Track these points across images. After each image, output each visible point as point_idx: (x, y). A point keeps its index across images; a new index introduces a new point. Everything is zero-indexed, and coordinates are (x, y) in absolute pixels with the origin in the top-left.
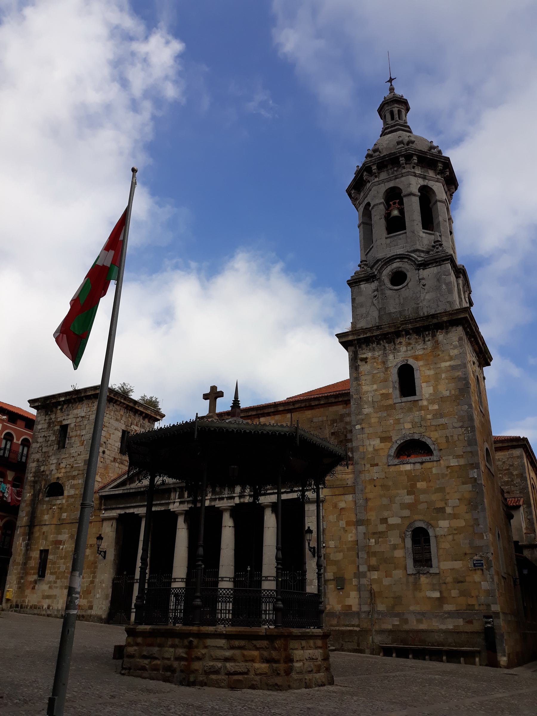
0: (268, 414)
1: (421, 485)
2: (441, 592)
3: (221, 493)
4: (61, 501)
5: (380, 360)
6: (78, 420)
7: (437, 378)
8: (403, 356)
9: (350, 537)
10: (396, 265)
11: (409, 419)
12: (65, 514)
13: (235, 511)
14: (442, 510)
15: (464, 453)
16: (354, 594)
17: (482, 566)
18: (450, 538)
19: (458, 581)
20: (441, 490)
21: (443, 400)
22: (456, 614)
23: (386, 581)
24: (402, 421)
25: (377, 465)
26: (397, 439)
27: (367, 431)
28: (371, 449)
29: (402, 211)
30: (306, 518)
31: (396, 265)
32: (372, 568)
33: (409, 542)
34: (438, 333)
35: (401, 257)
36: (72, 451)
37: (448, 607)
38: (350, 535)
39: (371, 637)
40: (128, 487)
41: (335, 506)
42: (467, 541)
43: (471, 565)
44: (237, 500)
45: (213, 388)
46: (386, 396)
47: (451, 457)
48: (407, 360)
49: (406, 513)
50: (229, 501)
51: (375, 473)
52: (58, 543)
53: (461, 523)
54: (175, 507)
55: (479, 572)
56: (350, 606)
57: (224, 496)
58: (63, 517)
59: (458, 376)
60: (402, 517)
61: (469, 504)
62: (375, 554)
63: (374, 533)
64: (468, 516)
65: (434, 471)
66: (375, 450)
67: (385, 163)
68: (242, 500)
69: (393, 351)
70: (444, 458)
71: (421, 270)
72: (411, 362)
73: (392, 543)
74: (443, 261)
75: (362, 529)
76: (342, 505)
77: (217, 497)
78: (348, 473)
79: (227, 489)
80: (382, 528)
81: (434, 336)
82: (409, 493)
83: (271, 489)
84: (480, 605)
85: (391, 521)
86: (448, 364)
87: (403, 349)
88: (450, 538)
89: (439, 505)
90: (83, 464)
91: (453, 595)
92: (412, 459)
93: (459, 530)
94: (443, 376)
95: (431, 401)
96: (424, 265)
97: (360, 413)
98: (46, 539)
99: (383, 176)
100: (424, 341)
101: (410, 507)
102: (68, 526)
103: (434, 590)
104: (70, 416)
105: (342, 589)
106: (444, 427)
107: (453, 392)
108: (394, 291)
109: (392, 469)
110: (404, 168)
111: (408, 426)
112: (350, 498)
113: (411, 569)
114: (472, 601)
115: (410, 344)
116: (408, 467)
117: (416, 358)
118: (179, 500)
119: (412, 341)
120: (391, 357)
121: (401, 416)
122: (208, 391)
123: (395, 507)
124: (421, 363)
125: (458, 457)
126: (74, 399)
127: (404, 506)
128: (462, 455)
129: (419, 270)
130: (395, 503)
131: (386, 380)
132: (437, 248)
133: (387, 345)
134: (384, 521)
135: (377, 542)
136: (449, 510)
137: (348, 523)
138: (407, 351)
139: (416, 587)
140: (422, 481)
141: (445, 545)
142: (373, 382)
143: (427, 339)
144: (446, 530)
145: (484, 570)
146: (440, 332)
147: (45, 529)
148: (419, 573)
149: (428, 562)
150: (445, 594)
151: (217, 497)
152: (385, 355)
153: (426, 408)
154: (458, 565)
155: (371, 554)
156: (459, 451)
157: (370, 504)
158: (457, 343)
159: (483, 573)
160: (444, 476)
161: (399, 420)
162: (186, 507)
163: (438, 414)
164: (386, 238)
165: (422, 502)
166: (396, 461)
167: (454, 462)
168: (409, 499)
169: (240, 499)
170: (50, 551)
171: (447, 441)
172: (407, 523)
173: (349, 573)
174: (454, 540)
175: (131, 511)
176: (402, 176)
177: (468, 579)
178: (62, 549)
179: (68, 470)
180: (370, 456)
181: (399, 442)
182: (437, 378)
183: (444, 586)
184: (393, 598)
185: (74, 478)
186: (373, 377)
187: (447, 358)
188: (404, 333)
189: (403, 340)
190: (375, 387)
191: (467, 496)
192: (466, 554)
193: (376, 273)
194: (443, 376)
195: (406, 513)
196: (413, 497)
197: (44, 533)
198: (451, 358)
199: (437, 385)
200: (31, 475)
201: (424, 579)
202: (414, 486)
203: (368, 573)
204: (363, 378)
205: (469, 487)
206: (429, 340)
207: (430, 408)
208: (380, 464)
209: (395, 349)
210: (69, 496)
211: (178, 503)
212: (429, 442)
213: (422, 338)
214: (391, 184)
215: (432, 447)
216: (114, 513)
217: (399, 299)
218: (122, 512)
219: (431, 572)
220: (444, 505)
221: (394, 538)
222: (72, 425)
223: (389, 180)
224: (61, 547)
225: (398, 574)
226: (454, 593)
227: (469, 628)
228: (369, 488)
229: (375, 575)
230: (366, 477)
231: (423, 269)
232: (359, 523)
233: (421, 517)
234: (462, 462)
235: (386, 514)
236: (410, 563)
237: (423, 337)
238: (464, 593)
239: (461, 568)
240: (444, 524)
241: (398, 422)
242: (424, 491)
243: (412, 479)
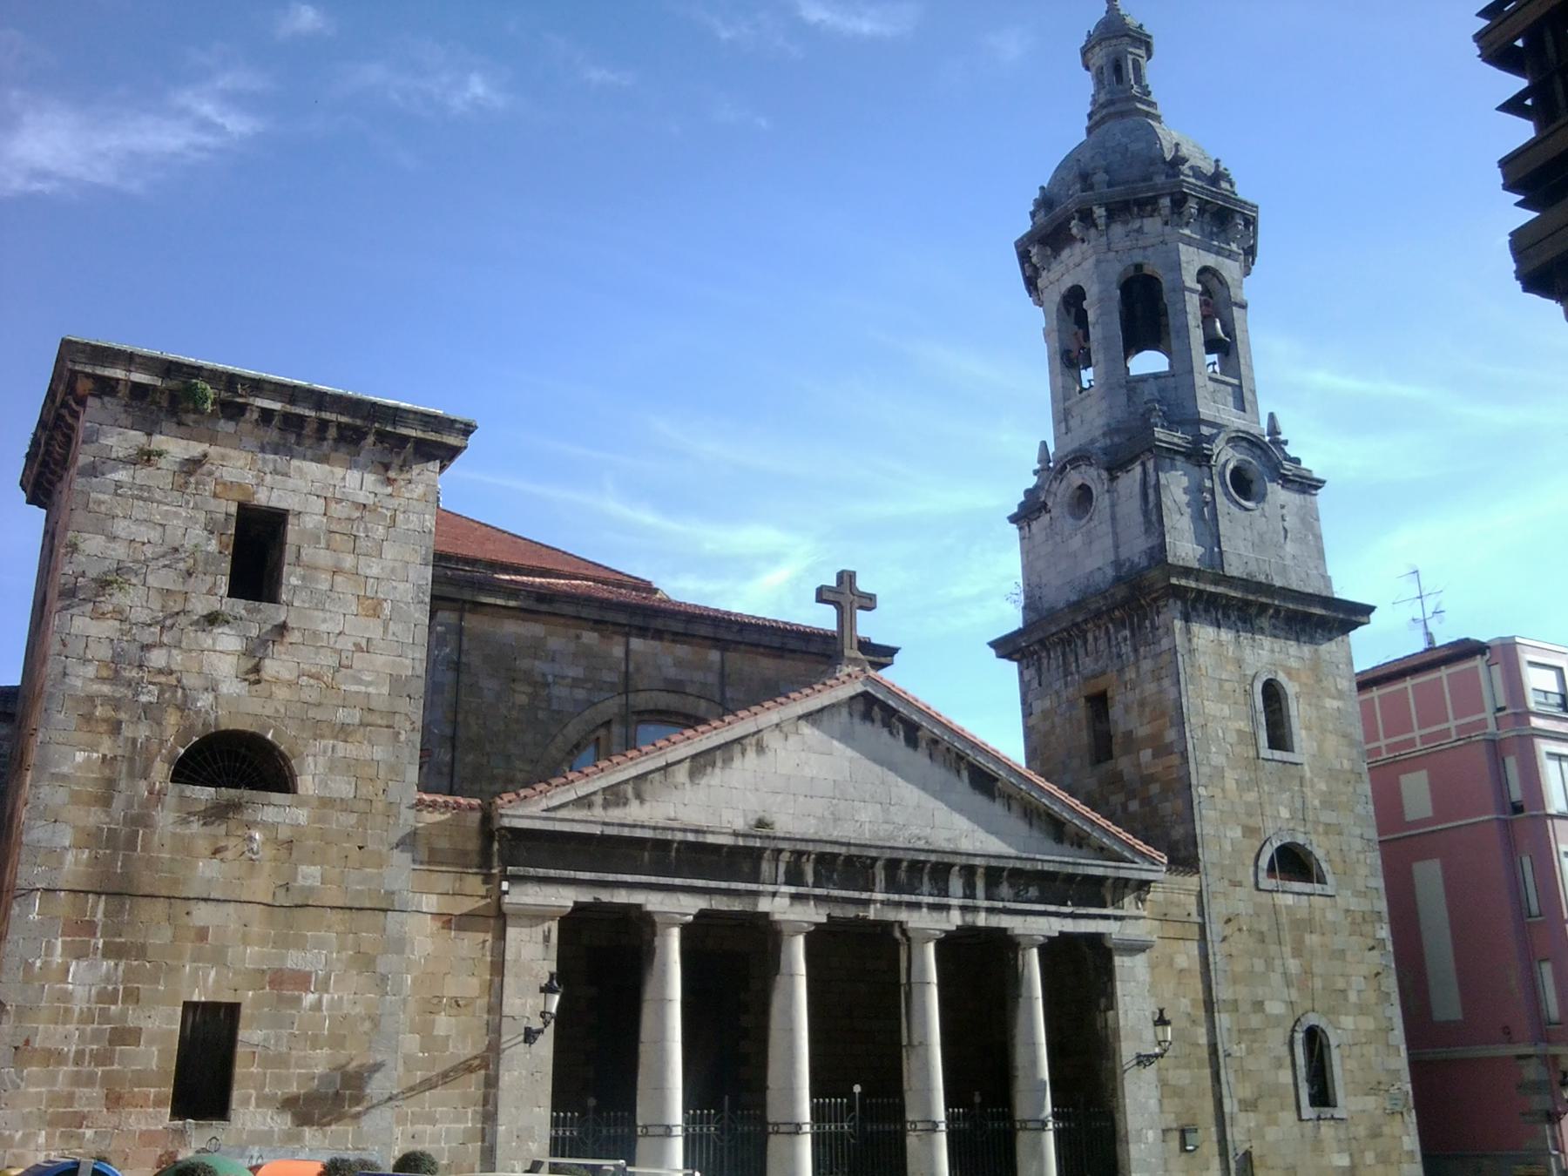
0: (659, 635)
4: (273, 811)
6: (337, 510)
12: (315, 870)
13: (949, 946)
19: (1375, 1134)
21: (1333, 775)
30: (1118, 984)
32: (1248, 1106)
36: (324, 627)
40: (598, 813)
44: (955, 920)
45: (847, 578)
50: (935, 915)
52: (285, 983)
54: (778, 905)
58: (300, 881)
68: (969, 918)
72: (1282, 677)
77: (906, 898)
79: (926, 879)
80: (1255, 1021)
89: (1341, 984)
90: (385, 690)
98: (218, 957)
102: (335, 916)
104: (291, 483)
116: (1289, 899)
118: (793, 890)
122: (863, 585)
126: (323, 425)
134: (1258, 1005)
135: (1250, 1051)
136: (1353, 997)
139: (1317, 1145)
147: (203, 915)
148: (1319, 1118)
151: (906, 898)
154: (1371, 1102)
162: (815, 915)
167: (1355, 904)
168: (1293, 965)
169: (963, 915)
170: (245, 1011)
175: (621, 897)
178: (317, 1006)
179: (310, 695)
185: (343, 732)
186: (1221, 687)
197: (202, 934)
200: (91, 671)
201: (1326, 1130)
203: (1241, 1117)
210: (326, 803)
211: (787, 901)
216: (565, 898)
218: (586, 896)
222: (311, 522)
224: (309, 999)
226: (1370, 1157)
235: (1260, 992)
240: (1348, 1022)
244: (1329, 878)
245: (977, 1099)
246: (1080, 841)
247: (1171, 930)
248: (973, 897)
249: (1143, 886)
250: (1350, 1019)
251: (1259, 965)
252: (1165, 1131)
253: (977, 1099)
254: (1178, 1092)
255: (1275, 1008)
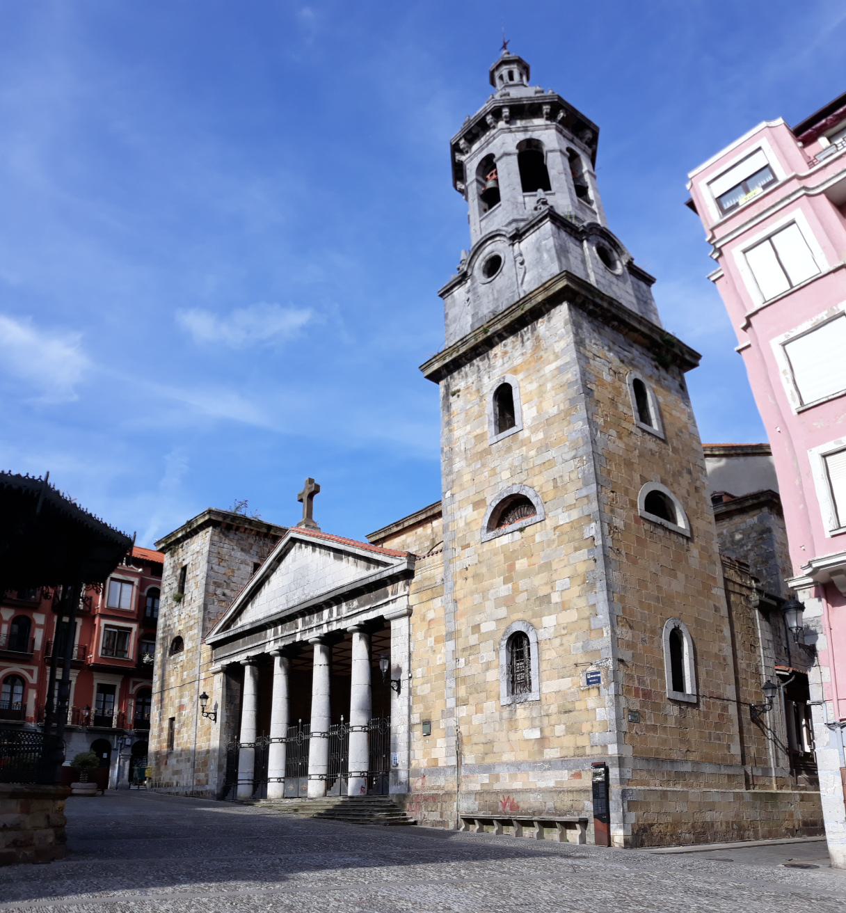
1: (521, 564)
2: (542, 731)
3: (311, 622)
5: (474, 389)
7: (541, 392)
8: (500, 373)
9: (439, 659)
10: (489, 249)
11: (506, 464)
14: (547, 598)
15: (577, 500)
16: (441, 742)
17: (599, 682)
18: (557, 642)
20: (547, 566)
22: (563, 762)
23: (477, 719)
24: (498, 470)
25: (468, 546)
26: (492, 500)
27: (457, 497)
28: (462, 524)
29: (496, 180)
31: (489, 249)
32: (461, 702)
33: (504, 656)
34: (539, 325)
35: (492, 237)
37: (551, 754)
38: (439, 656)
39: (455, 804)
41: (423, 619)
42: (580, 644)
43: (583, 682)
44: (325, 630)
46: (480, 438)
47: (560, 510)
48: (504, 378)
49: (502, 612)
51: (466, 558)
53: (571, 616)
55: (594, 692)
56: (436, 760)
57: (313, 626)
59: (567, 380)
60: (498, 620)
61: (584, 583)
62: (464, 679)
63: (464, 650)
64: (582, 603)
65: (538, 539)
66: (467, 524)
67: (474, 131)
69: (488, 370)
70: (550, 515)
71: (517, 244)
73: (484, 661)
74: (541, 221)
75: (451, 645)
76: (431, 615)
78: (436, 567)
80: (473, 639)
81: (534, 330)
82: (506, 581)
83: (358, 607)
84: (592, 746)
85: (485, 628)
86: (554, 366)
87: (498, 362)
88: (557, 642)
91: (557, 734)
92: (508, 528)
93: (568, 629)
94: (549, 386)
95: (534, 430)
96: (517, 237)
97: (450, 472)
99: (475, 147)
100: (523, 342)
101: (508, 602)
103: (533, 727)
105: (429, 735)
106: (549, 464)
107: (562, 407)
108: (487, 285)
109: (487, 546)
110: (494, 127)
111: (506, 475)
112: (438, 602)
113: (506, 700)
114: (583, 741)
115: (505, 353)
116: (505, 540)
117: (515, 371)
119: (509, 348)
120: (485, 380)
121: (496, 463)
123: (489, 605)
124: (520, 376)
125: (570, 507)
127: (500, 602)
128: (575, 504)
129: (513, 245)
130: (488, 600)
131: (480, 415)
132: (540, 209)
133: (480, 364)
134: (476, 628)
136: (555, 598)
137: (437, 641)
138: (504, 364)
140: (522, 558)
141: (550, 654)
142: (467, 422)
143: (525, 338)
144: (552, 630)
145: (602, 688)
146: (541, 322)
149: (526, 684)
150: (547, 733)
152: (480, 379)
153: (524, 443)
154: (566, 684)
155: (459, 680)
156: (570, 498)
157: (461, 607)
158: (563, 330)
159: (599, 695)
160: (550, 543)
161: (494, 469)
163: (545, 447)
164: (481, 221)
165: (522, 592)
166: (491, 534)
167: (563, 518)
168: (504, 590)
171: (555, 487)
172: (503, 628)
173: (435, 716)
174: (562, 645)
176: (494, 139)
177: (578, 705)
180: (460, 535)
181: (494, 505)
182: (541, 392)
183: (546, 720)
184: (483, 743)
187: (552, 357)
188: (496, 339)
189: (498, 350)
190: (468, 428)
191: (582, 568)
192: (576, 665)
193: (465, 270)
194: (549, 386)
195: (502, 612)
196: (510, 585)
198: (557, 357)
199: (541, 402)
202: (512, 567)
204: (455, 420)
205: (583, 554)
206: (528, 339)
207: (533, 440)
208: (472, 543)
209: (489, 366)
212: (530, 494)
213: (520, 339)
214: (484, 154)
215: (534, 501)
217: (493, 295)
219: (530, 699)
220: (550, 591)
221: (487, 654)
223: (481, 149)
225: (490, 706)
226: (560, 730)
227: (577, 784)
228: (460, 582)
229: (463, 712)
230: (458, 566)
231: (519, 242)
232: (451, 635)
233: (520, 615)
234: (575, 515)
235: (478, 619)
236: (503, 687)
237: (522, 336)
238: (572, 730)
239: (570, 688)
240: (549, 621)
241: (494, 472)
242: (526, 574)
243: (511, 557)
244: (538, 509)
245: (342, 719)
246: (378, 563)
247: (425, 596)
248: (332, 616)
249: (408, 575)
250: (553, 617)
251: (477, 598)
252: (410, 727)
253: (342, 719)
254: (423, 698)
255: (487, 627)
